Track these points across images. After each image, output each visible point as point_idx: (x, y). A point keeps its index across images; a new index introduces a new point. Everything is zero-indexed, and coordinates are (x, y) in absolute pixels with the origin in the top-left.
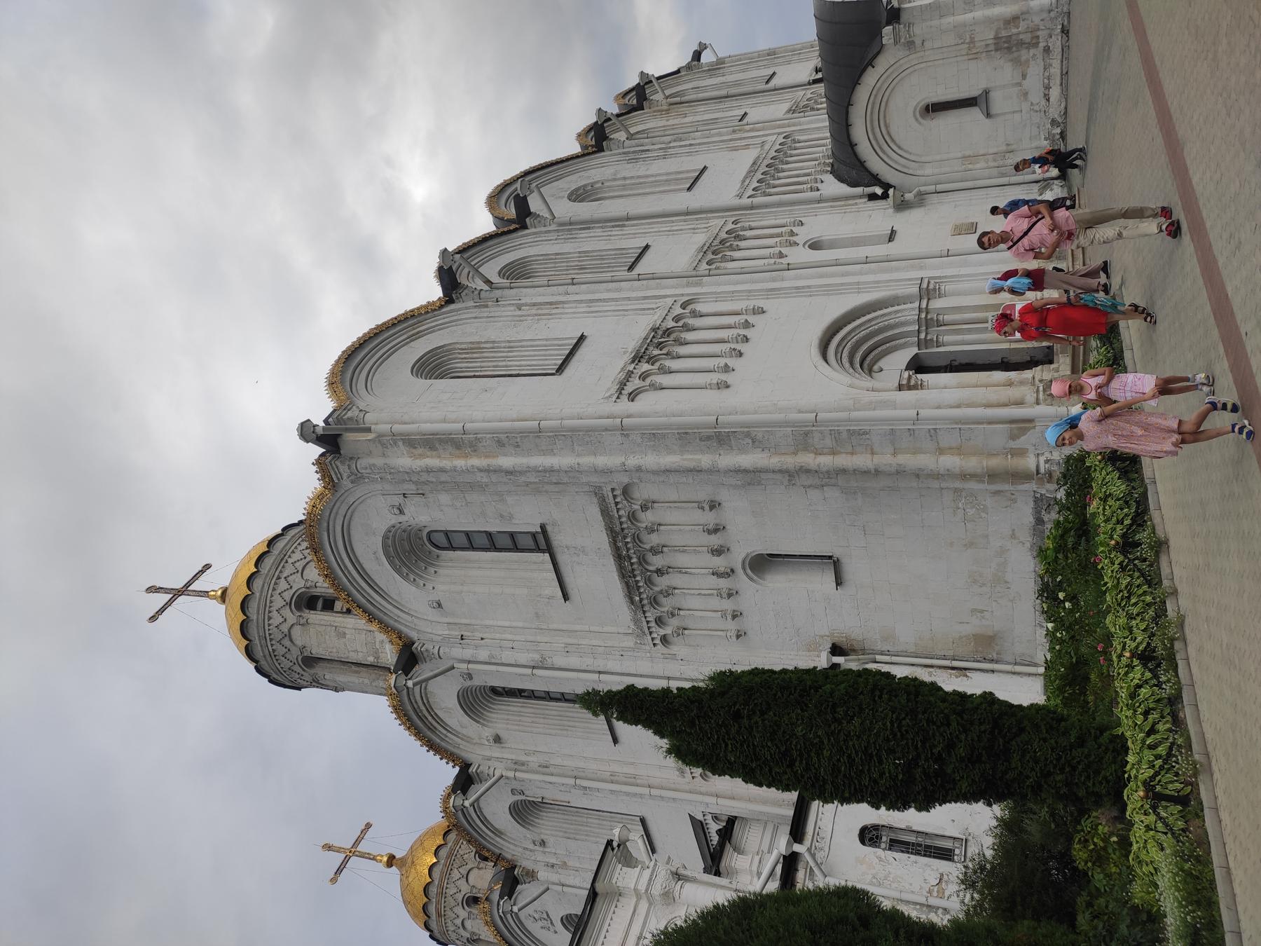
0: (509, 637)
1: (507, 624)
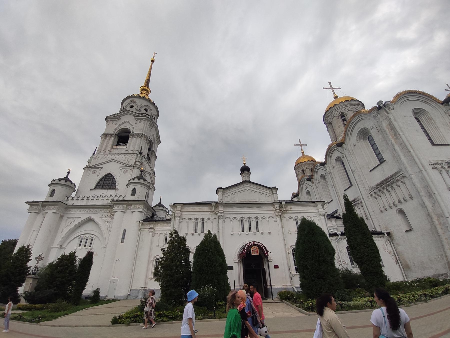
0: (355, 162)
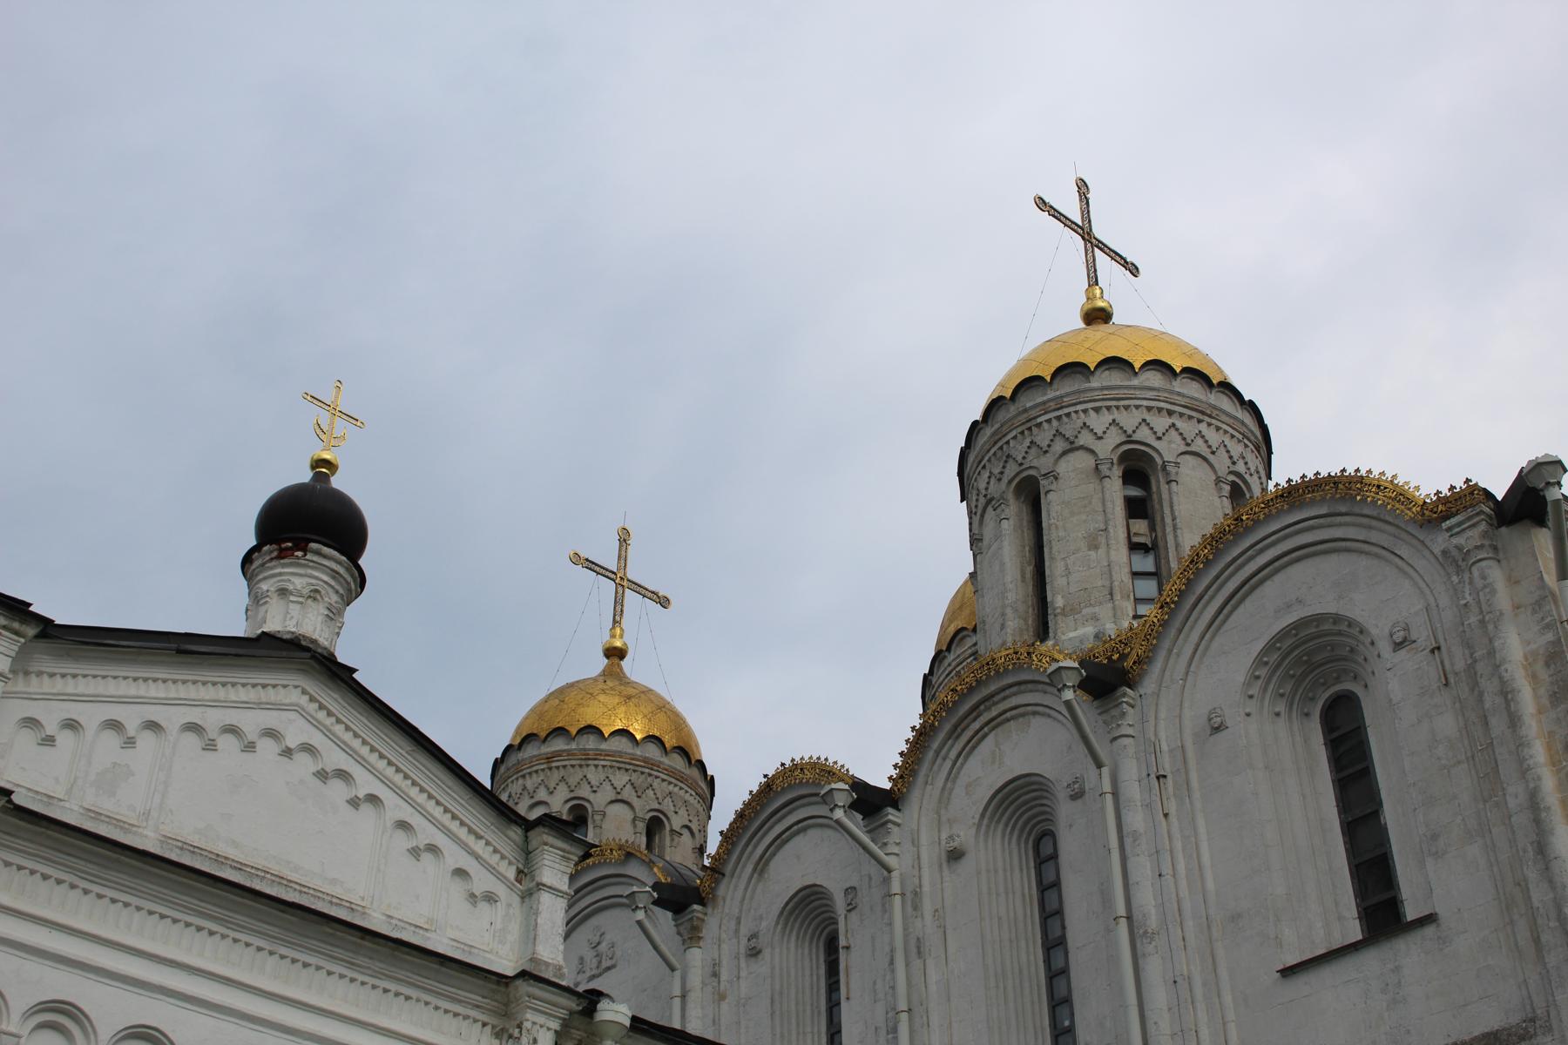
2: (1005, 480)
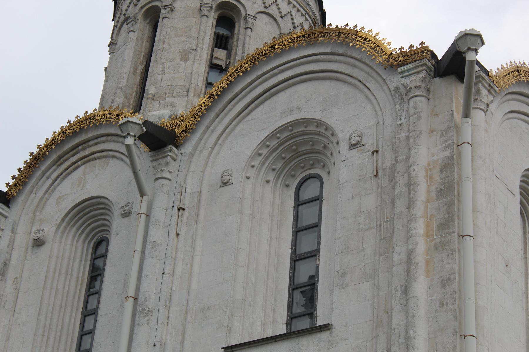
0: (179, 270)
1: (196, 268)
2: (140, 5)
